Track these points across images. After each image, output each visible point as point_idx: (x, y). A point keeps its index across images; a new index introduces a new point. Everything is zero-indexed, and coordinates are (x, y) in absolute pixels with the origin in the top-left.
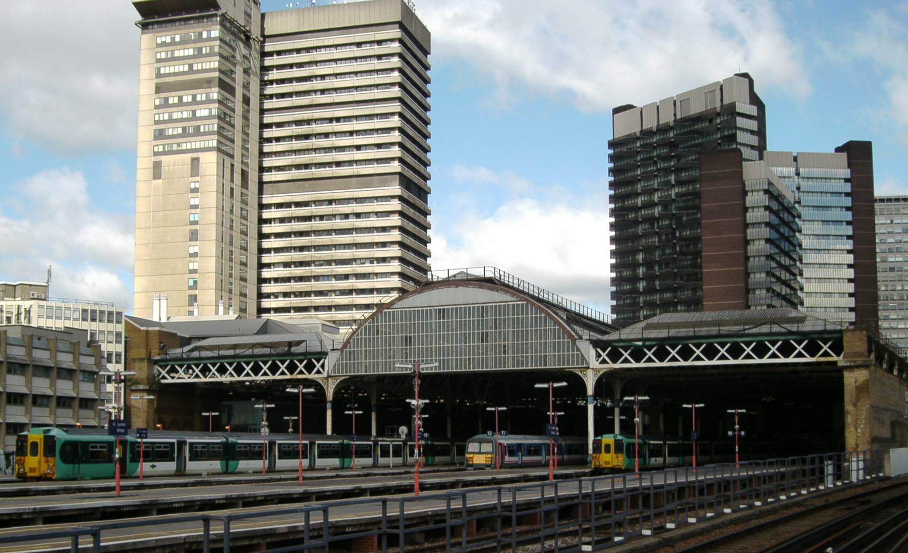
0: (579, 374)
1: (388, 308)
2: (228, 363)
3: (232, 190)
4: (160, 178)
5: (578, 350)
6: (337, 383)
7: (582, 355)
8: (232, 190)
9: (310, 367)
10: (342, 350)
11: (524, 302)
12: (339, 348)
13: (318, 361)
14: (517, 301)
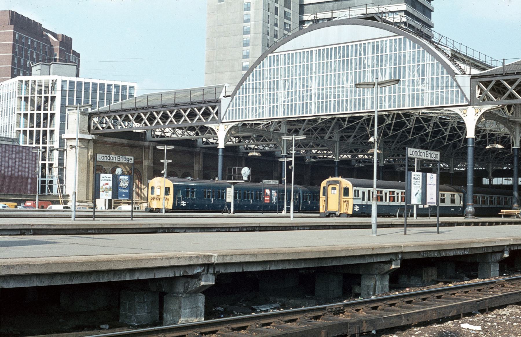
0: (459, 112)
1: (272, 53)
2: (143, 113)
3: (276, 9)
4: (223, 1)
5: (458, 86)
6: (228, 129)
7: (461, 90)
8: (276, 9)
9: (206, 114)
10: (232, 96)
11: (402, 37)
12: (230, 95)
13: (213, 108)
14: (394, 36)
